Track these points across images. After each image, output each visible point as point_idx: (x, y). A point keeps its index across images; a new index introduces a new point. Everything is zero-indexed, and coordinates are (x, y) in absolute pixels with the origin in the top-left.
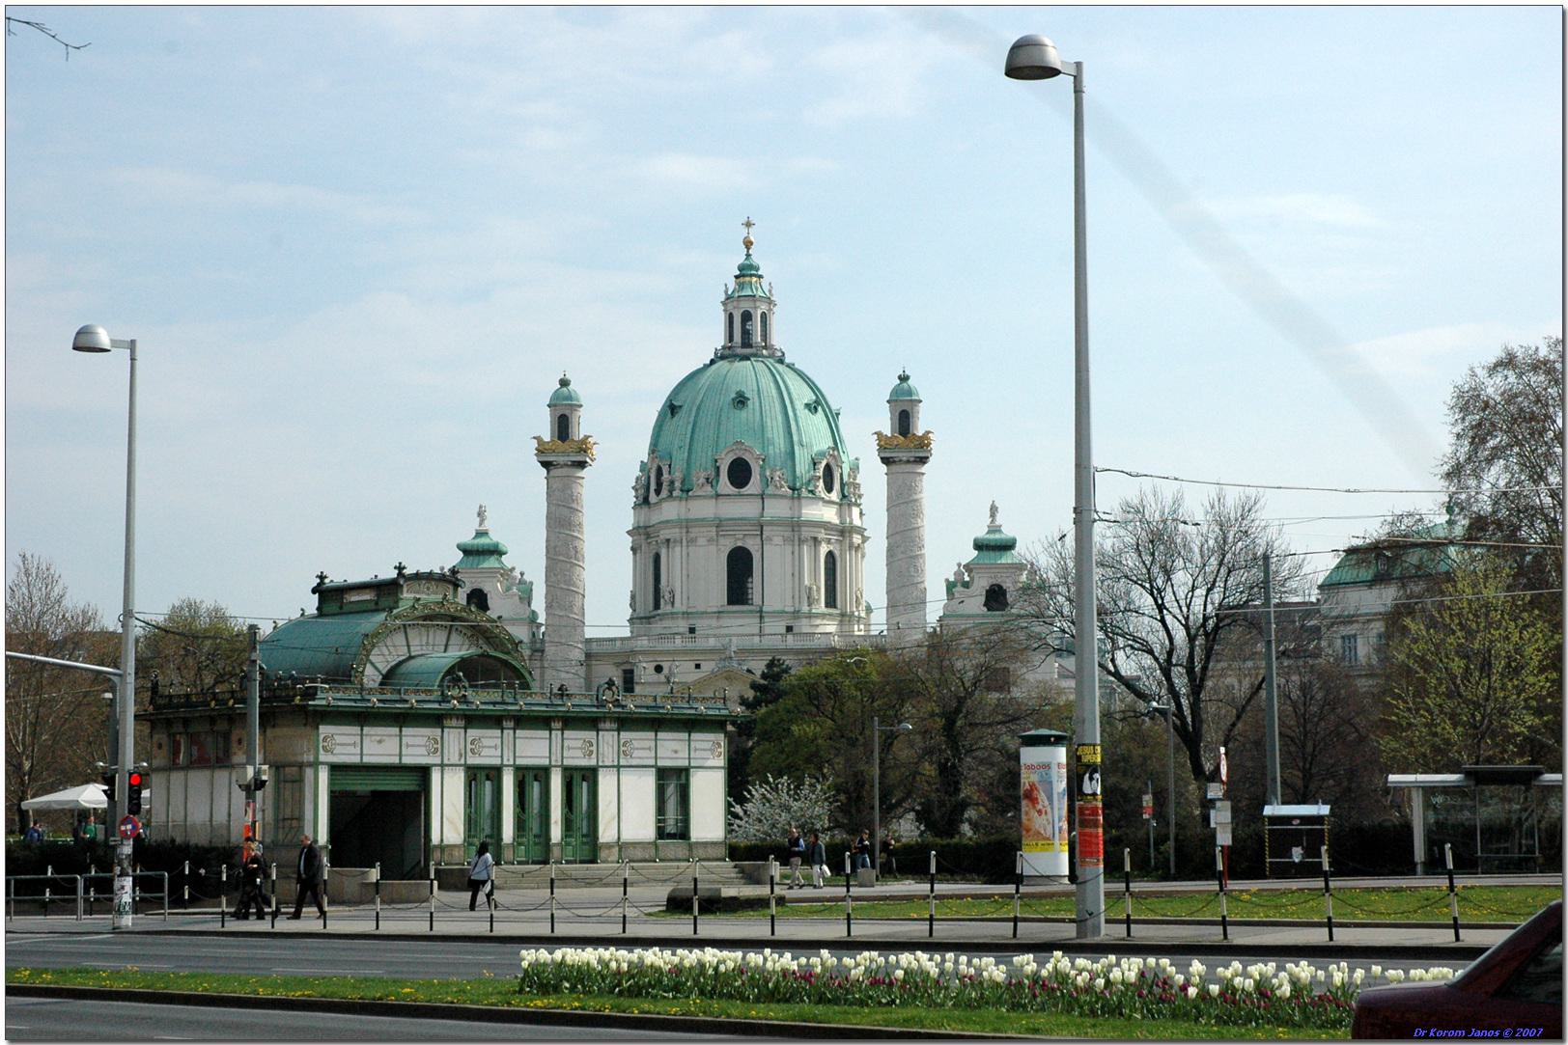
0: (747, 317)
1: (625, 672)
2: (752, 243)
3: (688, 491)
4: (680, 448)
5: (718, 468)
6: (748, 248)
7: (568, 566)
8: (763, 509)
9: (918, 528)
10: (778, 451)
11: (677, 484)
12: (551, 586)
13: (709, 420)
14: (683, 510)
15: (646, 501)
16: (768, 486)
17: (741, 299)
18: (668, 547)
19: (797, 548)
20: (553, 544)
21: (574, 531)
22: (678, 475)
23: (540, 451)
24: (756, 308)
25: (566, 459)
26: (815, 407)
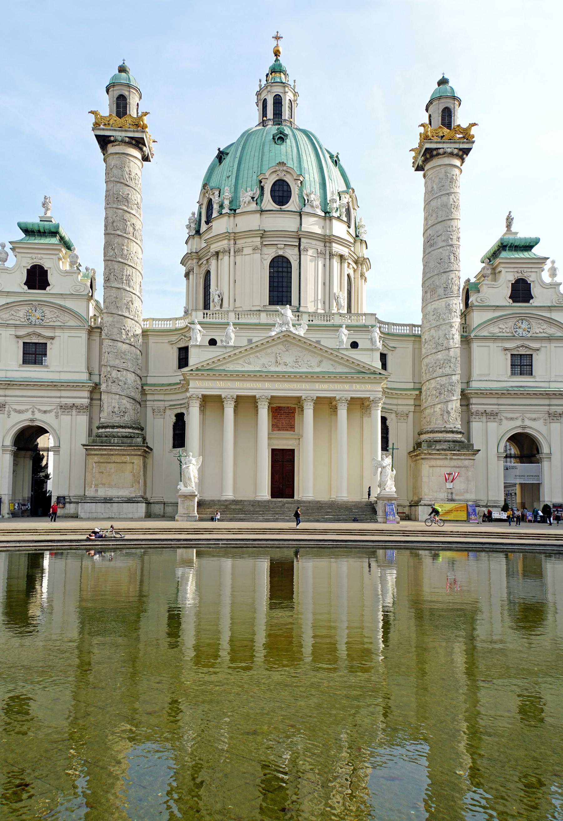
0: (278, 101)
1: (180, 349)
2: (280, 53)
6: (276, 55)
8: (301, 224)
9: (457, 219)
10: (312, 179)
11: (227, 202)
12: (108, 260)
13: (253, 153)
16: (305, 205)
20: (110, 220)
21: (132, 209)
23: (96, 126)
24: (285, 93)
25: (124, 134)
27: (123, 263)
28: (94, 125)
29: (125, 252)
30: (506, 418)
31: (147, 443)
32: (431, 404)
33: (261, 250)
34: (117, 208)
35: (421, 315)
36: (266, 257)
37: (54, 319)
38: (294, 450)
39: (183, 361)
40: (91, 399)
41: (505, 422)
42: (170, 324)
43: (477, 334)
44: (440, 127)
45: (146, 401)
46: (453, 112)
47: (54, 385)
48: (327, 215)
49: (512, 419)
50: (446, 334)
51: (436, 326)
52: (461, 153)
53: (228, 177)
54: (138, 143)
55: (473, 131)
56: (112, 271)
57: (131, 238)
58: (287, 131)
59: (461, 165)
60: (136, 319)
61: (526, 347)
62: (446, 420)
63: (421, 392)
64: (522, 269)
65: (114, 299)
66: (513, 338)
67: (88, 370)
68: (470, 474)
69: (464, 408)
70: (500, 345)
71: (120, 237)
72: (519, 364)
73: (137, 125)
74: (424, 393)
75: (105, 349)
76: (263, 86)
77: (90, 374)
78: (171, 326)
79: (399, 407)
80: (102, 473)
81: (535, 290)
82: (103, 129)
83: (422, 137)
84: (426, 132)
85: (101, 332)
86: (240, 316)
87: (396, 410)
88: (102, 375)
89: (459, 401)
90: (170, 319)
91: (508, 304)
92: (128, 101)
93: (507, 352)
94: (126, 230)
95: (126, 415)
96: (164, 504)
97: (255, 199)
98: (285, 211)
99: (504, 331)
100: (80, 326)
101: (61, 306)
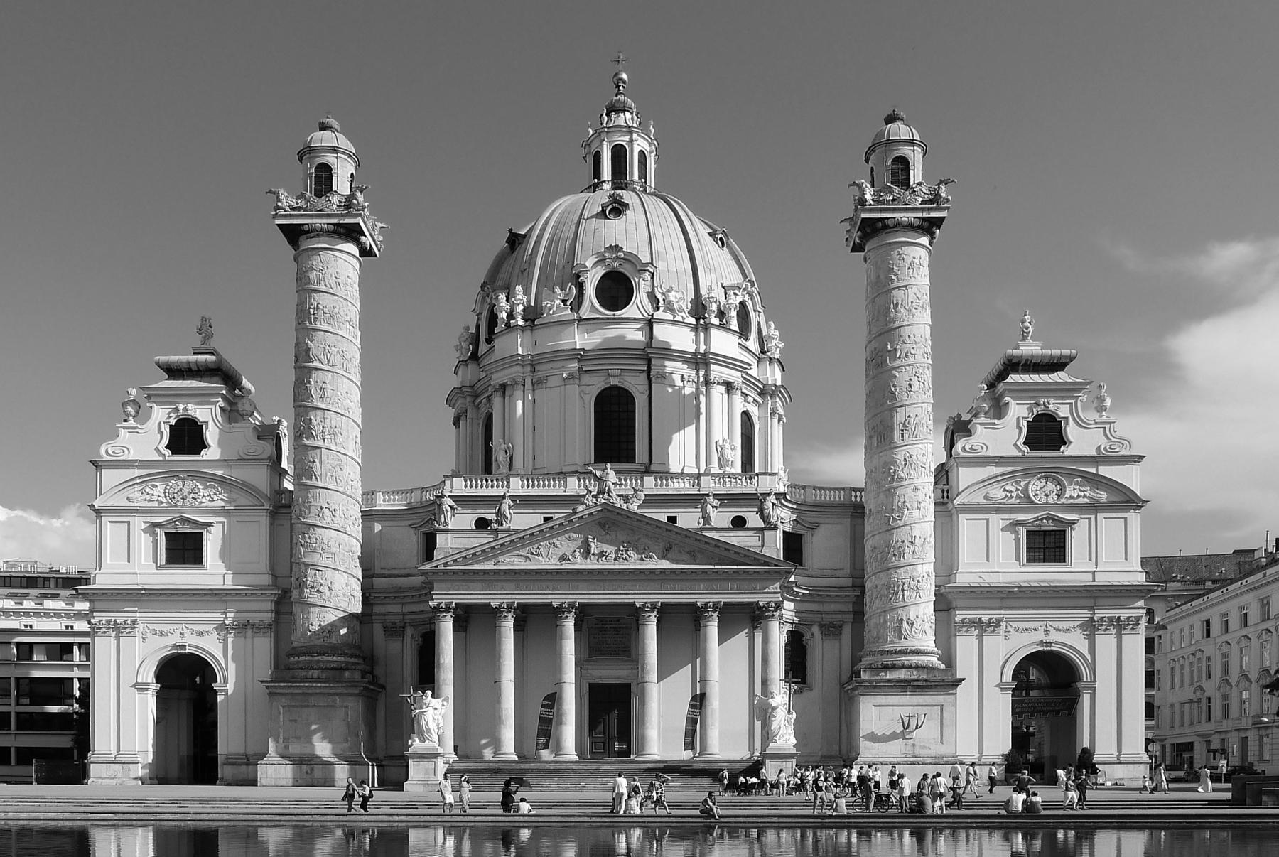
0: (619, 155)
3: (533, 321)
4: (522, 272)
17: (613, 129)
24: (631, 141)
32: (879, 611)
35: (863, 472)
39: (429, 556)
43: (966, 501)
48: (702, 322)
58: (627, 196)
70: (1006, 516)
72: (1042, 545)
80: (296, 721)
90: (412, 491)
97: (568, 303)
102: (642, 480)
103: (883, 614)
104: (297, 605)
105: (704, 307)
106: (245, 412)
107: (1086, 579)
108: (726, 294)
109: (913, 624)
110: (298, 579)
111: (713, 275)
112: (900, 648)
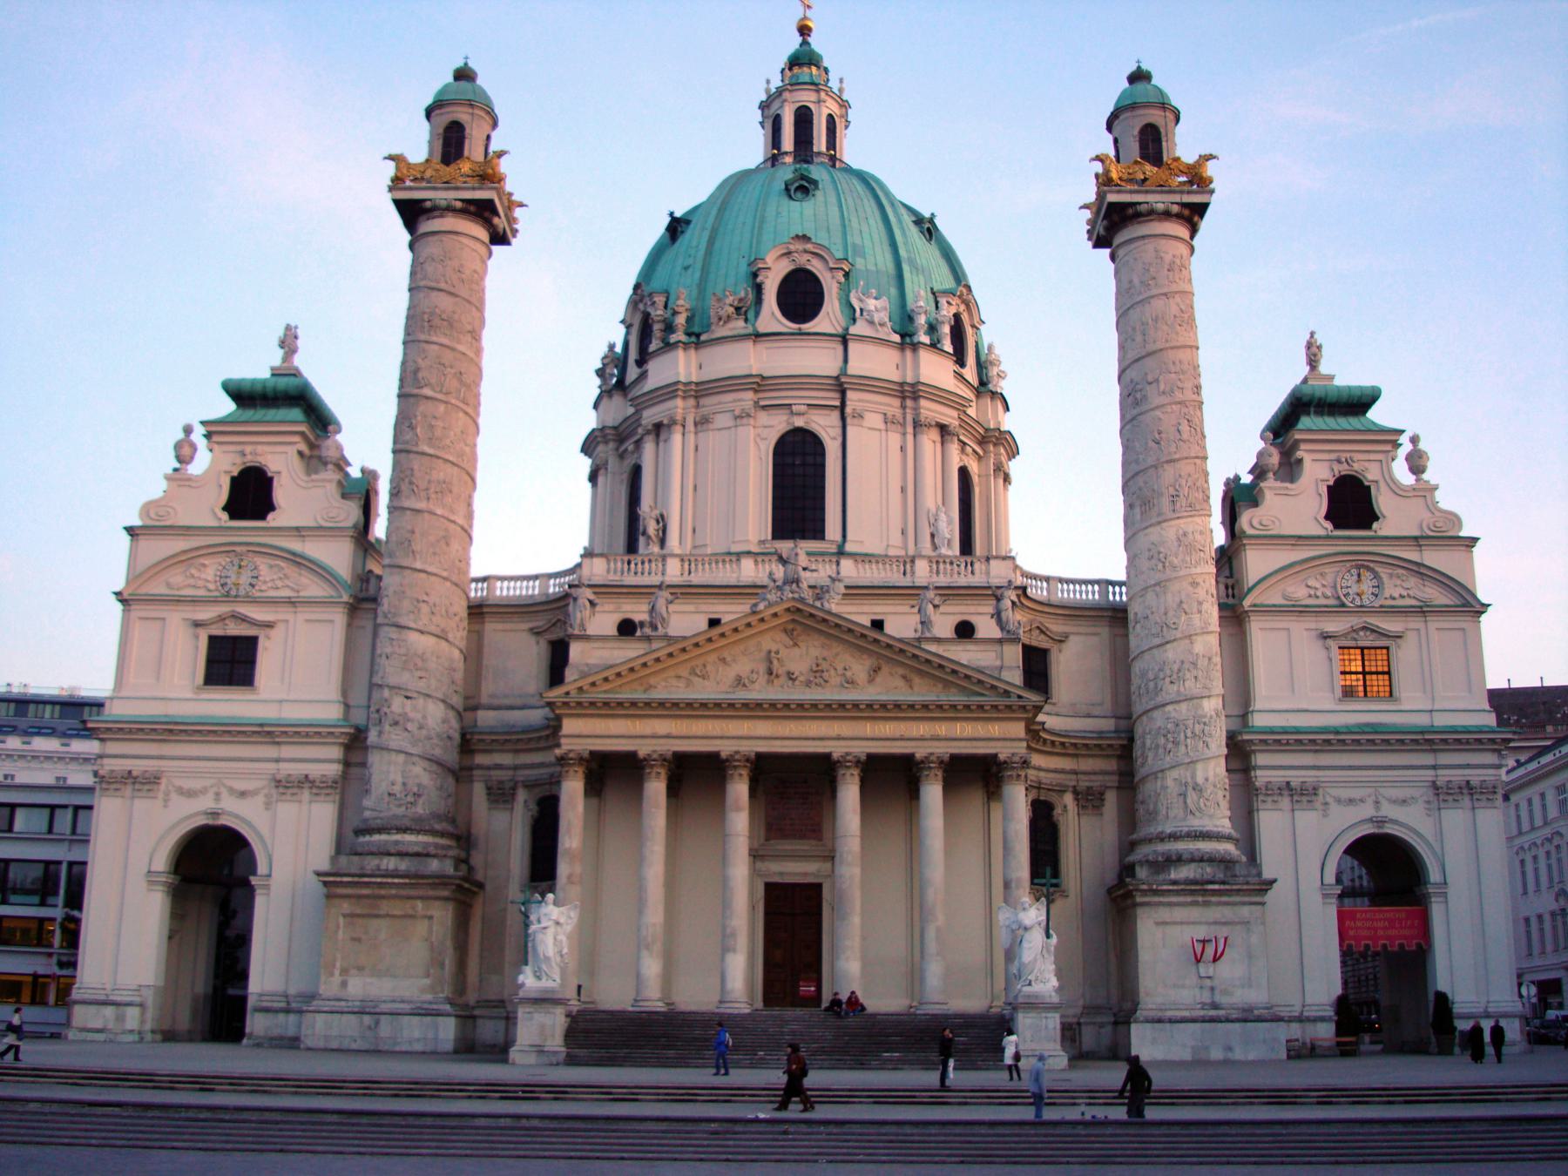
3: (698, 336)
4: (686, 268)
5: (758, 289)
7: (442, 408)
8: (846, 360)
11: (681, 320)
12: (401, 451)
14: (694, 365)
15: (621, 386)
16: (854, 320)
18: (657, 444)
19: (910, 438)
21: (459, 342)
22: (683, 303)
23: (397, 183)
24: (819, 102)
25: (452, 195)
26: (929, 230)
27: (431, 455)
28: (393, 181)
29: (438, 433)
30: (1339, 801)
31: (471, 869)
32: (1154, 770)
33: (754, 418)
34: (427, 342)
36: (765, 433)
37: (279, 584)
38: (818, 887)
40: (347, 764)
41: (1334, 807)
42: (534, 588)
43: (1258, 601)
44: (1136, 162)
45: (471, 769)
46: (1162, 130)
47: (266, 733)
49: (1351, 801)
50: (1181, 602)
51: (1158, 584)
52: (1186, 212)
53: (686, 268)
54: (482, 211)
55: (1211, 169)
56: (408, 473)
57: (453, 401)
59: (1192, 237)
60: (454, 578)
61: (1373, 631)
62: (1194, 809)
63: (1131, 740)
64: (1348, 455)
65: (408, 535)
66: (1341, 608)
67: (345, 693)
68: (1254, 939)
69: (1238, 777)
71: (430, 402)
72: (1360, 669)
73: (480, 176)
74: (1138, 743)
75: (384, 647)
76: (774, 90)
77: (347, 706)
78: (536, 592)
79: (1080, 776)
81: (1383, 501)
82: (410, 189)
83: (1100, 180)
84: (1107, 172)
85: (375, 610)
86: (693, 565)
87: (1074, 783)
88: (372, 709)
89: (1223, 761)
90: (536, 577)
91: (1322, 532)
92: (468, 131)
93: (1330, 642)
94: (442, 386)
95: (421, 801)
96: (507, 1018)
98: (809, 334)
99: (1319, 594)
100: (332, 597)
101: (294, 554)
102: (838, 563)
103: (1160, 775)
104: (375, 751)
105: (911, 319)
106: (329, 459)
107: (1422, 720)
108: (937, 303)
109: (1201, 791)
110: (378, 711)
111: (921, 277)
112: (1186, 829)
